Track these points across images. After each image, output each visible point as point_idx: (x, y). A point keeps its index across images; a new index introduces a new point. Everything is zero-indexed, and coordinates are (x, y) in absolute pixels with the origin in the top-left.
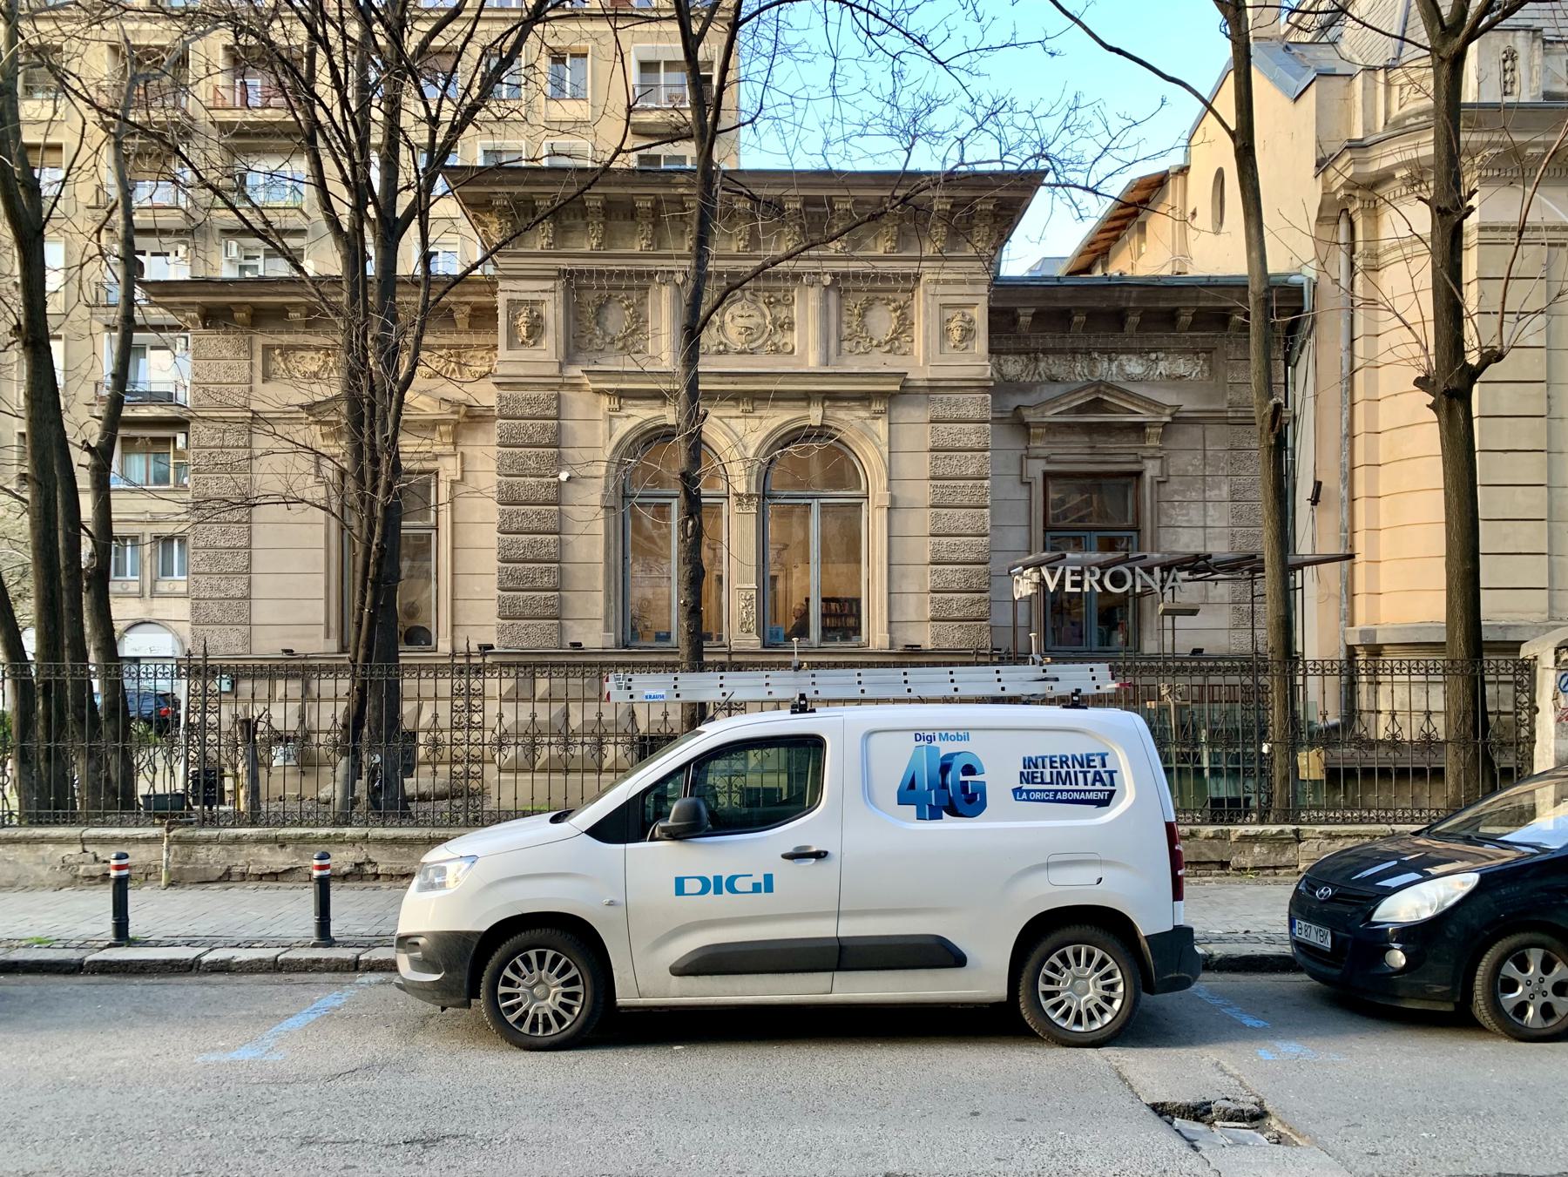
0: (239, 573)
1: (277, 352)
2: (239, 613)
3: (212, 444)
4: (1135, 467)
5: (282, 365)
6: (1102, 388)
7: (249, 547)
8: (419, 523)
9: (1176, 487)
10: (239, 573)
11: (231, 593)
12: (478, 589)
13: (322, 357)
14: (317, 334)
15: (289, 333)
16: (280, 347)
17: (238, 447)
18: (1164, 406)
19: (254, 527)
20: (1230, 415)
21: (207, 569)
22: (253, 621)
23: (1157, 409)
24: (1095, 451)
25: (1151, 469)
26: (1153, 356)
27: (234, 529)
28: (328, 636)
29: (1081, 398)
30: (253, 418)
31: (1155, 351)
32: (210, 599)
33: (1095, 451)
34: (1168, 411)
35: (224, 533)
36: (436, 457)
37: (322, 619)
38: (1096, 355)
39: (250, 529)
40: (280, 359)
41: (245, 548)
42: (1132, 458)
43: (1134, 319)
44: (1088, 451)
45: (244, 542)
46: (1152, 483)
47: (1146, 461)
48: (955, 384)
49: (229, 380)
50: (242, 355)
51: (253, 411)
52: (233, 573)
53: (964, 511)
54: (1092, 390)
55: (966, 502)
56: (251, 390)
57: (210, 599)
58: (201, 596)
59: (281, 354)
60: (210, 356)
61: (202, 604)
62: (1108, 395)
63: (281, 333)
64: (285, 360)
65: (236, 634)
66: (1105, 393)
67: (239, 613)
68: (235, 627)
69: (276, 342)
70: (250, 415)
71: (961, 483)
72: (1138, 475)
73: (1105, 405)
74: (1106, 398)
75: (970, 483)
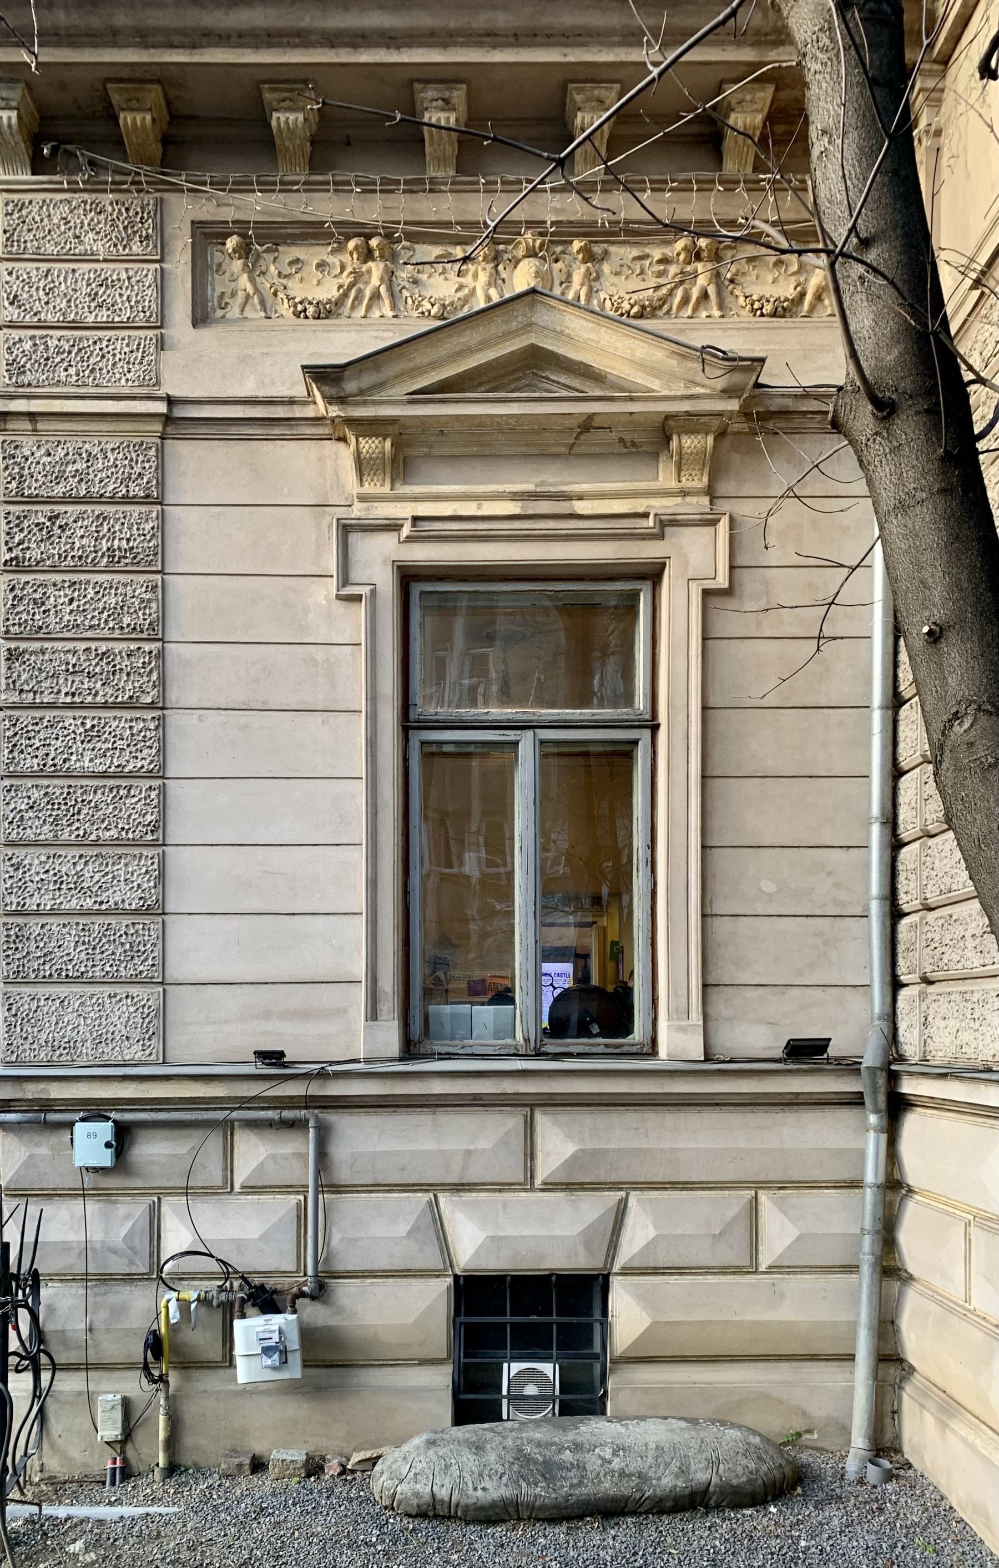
0: (134, 844)
1: (231, 243)
2: (133, 953)
3: (59, 490)
5: (244, 281)
7: (159, 773)
8: (607, 713)
10: (134, 844)
11: (113, 897)
12: (768, 886)
13: (351, 262)
14: (340, 187)
15: (266, 187)
16: (241, 227)
17: (127, 500)
19: (174, 718)
21: (46, 833)
22: (174, 972)
27: (118, 722)
28: (373, 1014)
30: (168, 419)
32: (52, 913)
35: (91, 735)
36: (666, 524)
37: (360, 969)
39: (161, 722)
40: (238, 264)
41: (150, 775)
45: (145, 760)
49: (103, 316)
50: (136, 248)
51: (171, 401)
52: (117, 843)
56: (161, 344)
57: (52, 913)
58: (31, 904)
59: (244, 251)
60: (50, 249)
61: (34, 925)
63: (242, 187)
64: (253, 270)
65: (126, 1008)
67: (133, 953)
68: (121, 990)
69: (229, 214)
70: (161, 408)
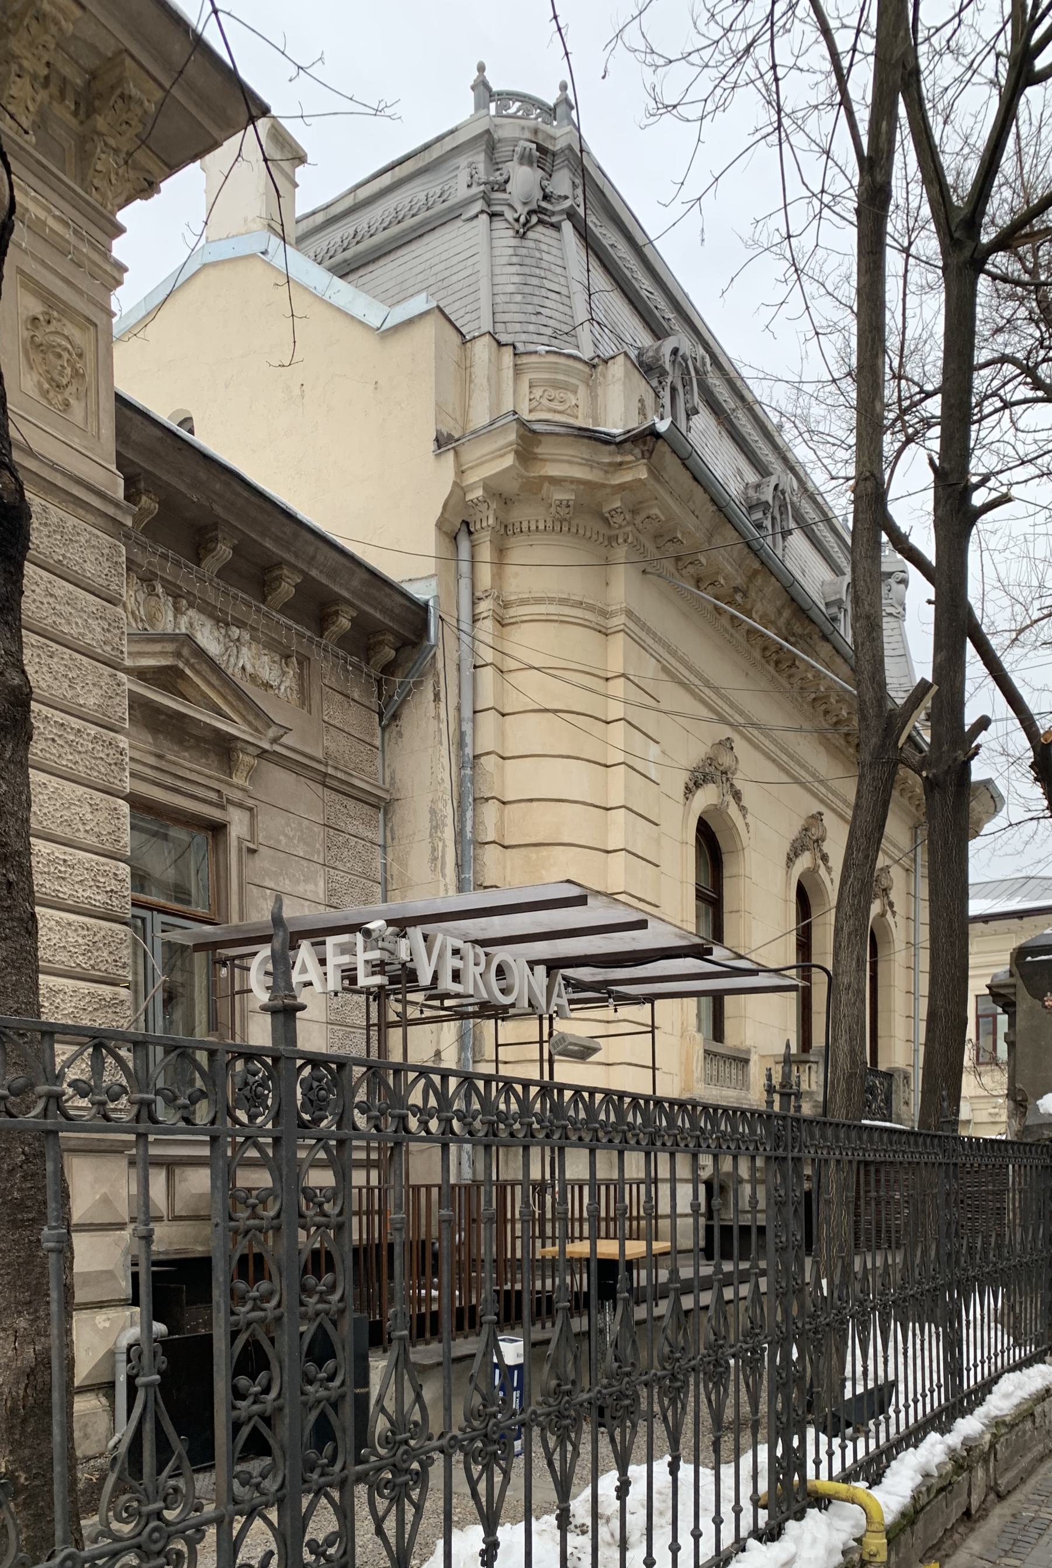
4: (215, 814)
6: (185, 652)
9: (266, 864)
18: (270, 722)
20: (330, 771)
23: (258, 724)
24: (163, 765)
25: (238, 826)
26: (235, 632)
29: (153, 654)
31: (241, 624)
33: (163, 765)
34: (272, 732)
38: (160, 590)
42: (213, 796)
43: (224, 551)
44: (152, 760)
46: (240, 850)
47: (231, 809)
48: (59, 481)
53: (81, 790)
54: (170, 647)
55: (81, 771)
62: (192, 667)
66: (187, 663)
71: (76, 723)
72: (217, 830)
73: (182, 685)
74: (188, 671)
75: (93, 730)
